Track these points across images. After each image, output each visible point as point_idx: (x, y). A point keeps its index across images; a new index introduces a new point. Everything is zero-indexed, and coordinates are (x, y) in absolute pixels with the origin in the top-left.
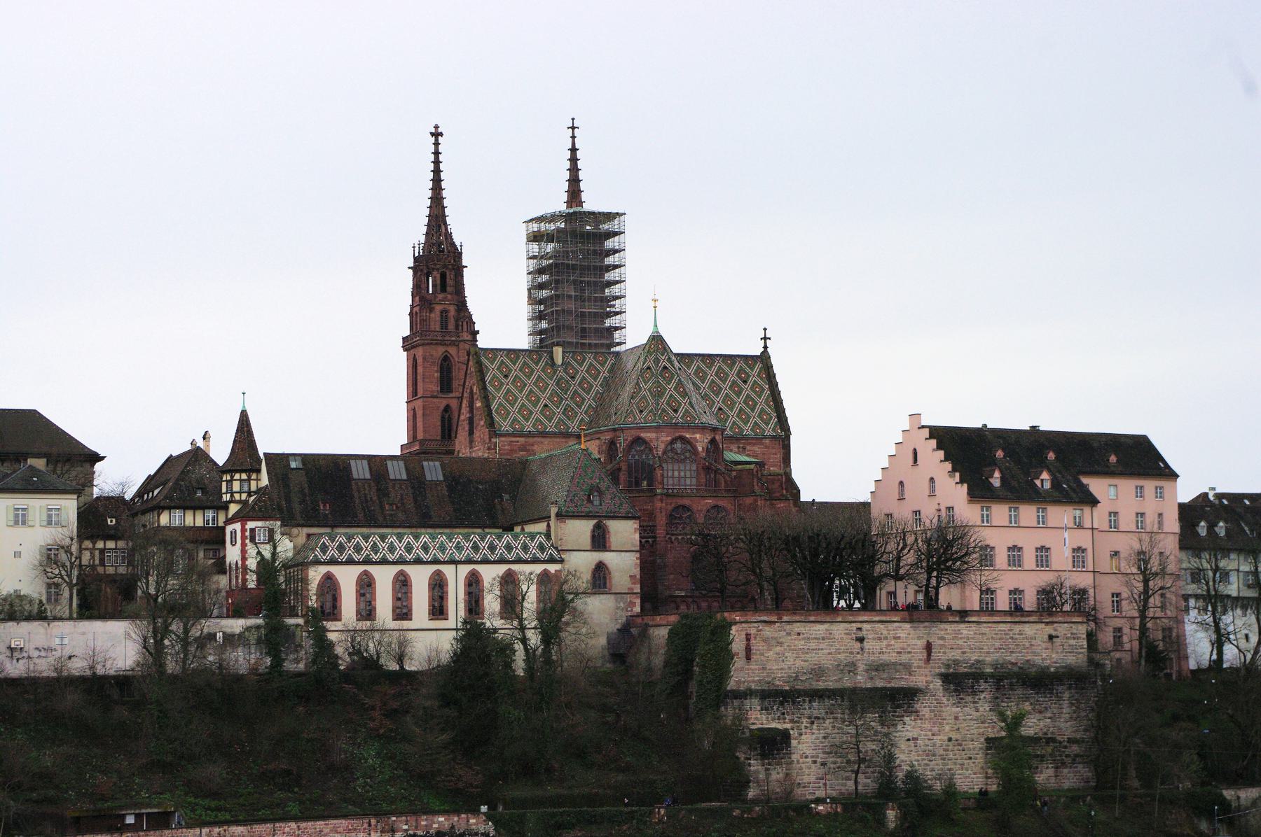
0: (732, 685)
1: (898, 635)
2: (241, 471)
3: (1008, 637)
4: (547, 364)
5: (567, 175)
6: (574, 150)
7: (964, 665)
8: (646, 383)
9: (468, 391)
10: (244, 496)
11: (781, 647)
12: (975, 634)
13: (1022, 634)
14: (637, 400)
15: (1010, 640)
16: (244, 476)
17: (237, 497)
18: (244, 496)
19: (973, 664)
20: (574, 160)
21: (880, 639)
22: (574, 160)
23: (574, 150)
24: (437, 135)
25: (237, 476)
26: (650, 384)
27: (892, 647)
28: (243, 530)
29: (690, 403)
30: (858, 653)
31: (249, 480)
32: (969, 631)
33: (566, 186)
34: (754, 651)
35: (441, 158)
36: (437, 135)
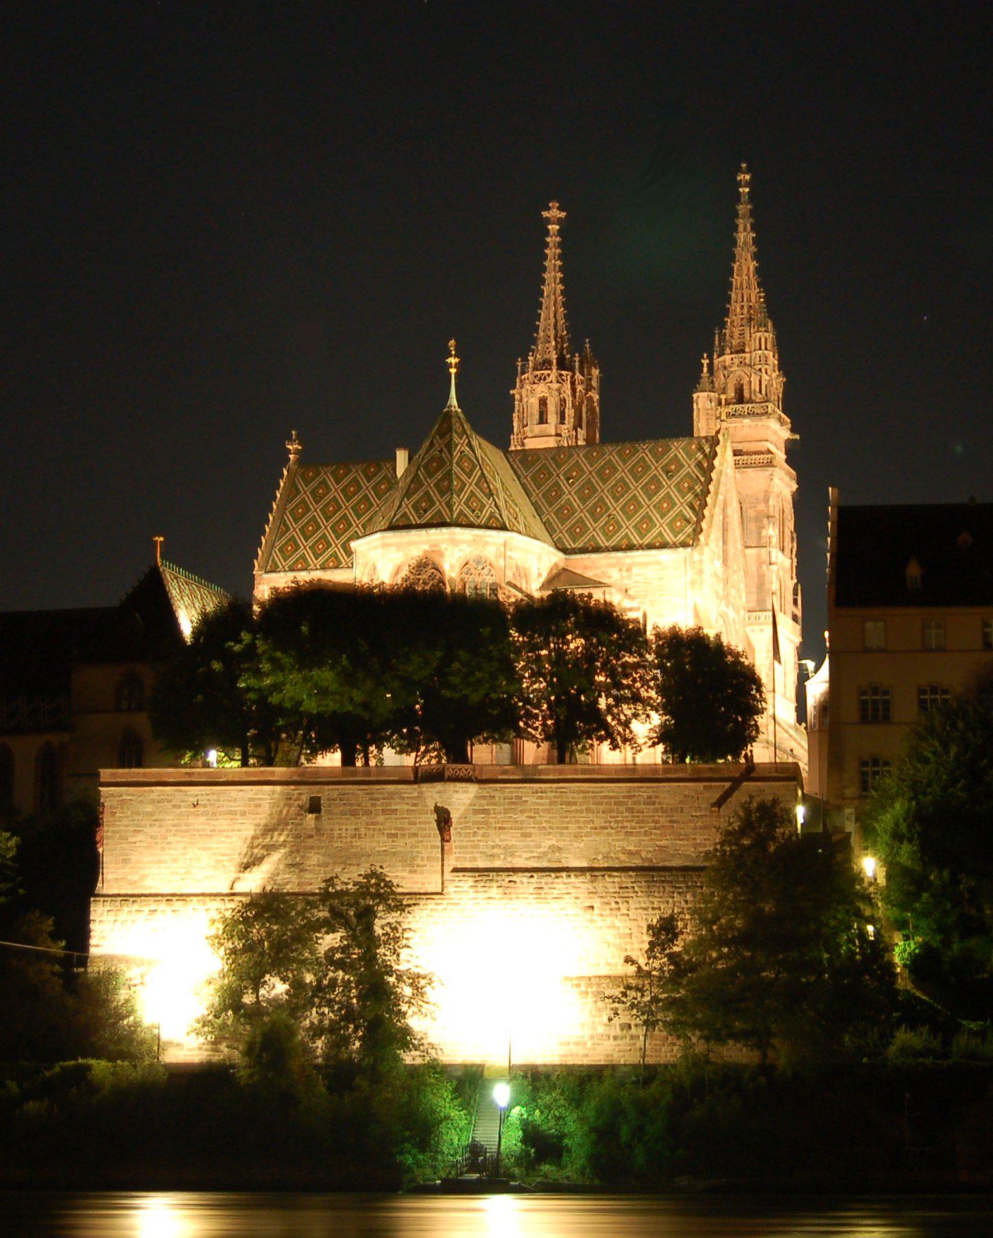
0: (96, 892)
1: (393, 807)
3: (623, 808)
4: (385, 478)
7: (525, 855)
11: (161, 826)
12: (551, 804)
13: (654, 803)
15: (626, 814)
19: (545, 854)
21: (354, 814)
27: (378, 827)
29: (496, 505)
30: (311, 836)
32: (541, 798)
34: (109, 834)
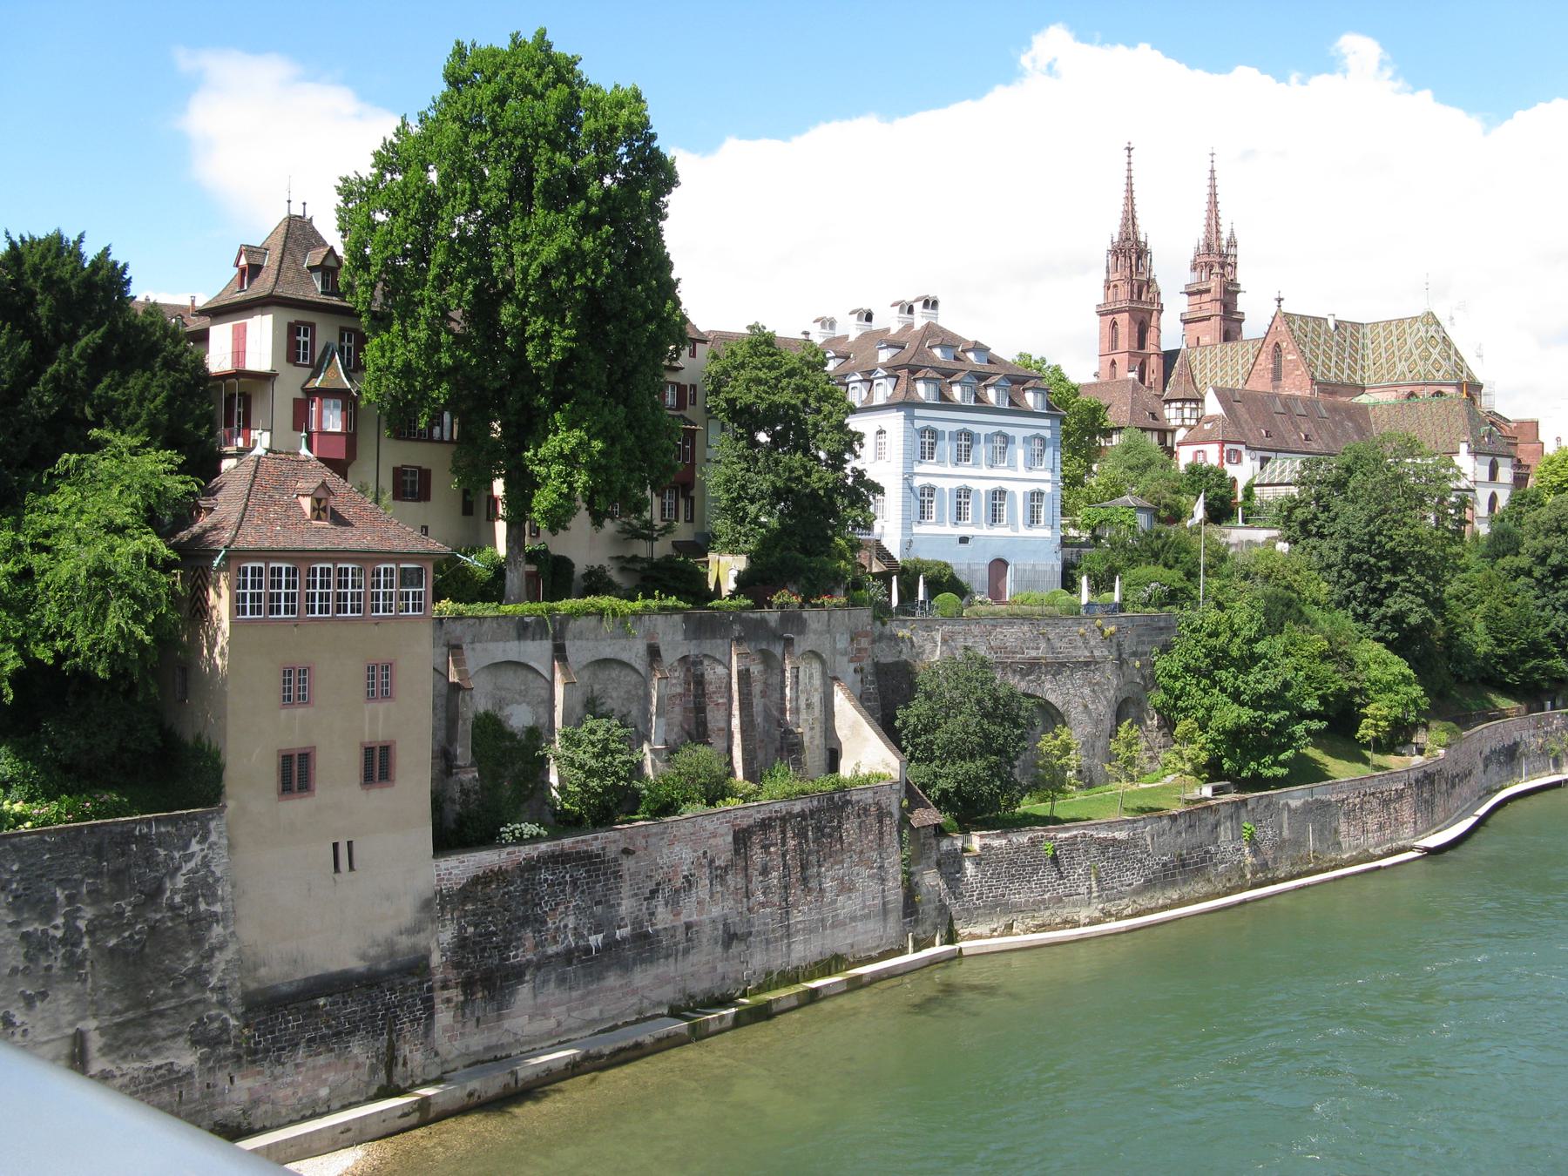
2: (1191, 400)
5: (1208, 190)
6: (1212, 171)
8: (1434, 348)
9: (1271, 346)
10: (1193, 422)
14: (1431, 361)
16: (1194, 405)
17: (1187, 422)
18: (1193, 422)
20: (1213, 178)
22: (1213, 178)
23: (1212, 171)
24: (1129, 149)
25: (1188, 405)
26: (1438, 349)
28: (1222, 451)
31: (1197, 409)
33: (1207, 199)
35: (1132, 166)
36: (1129, 149)
